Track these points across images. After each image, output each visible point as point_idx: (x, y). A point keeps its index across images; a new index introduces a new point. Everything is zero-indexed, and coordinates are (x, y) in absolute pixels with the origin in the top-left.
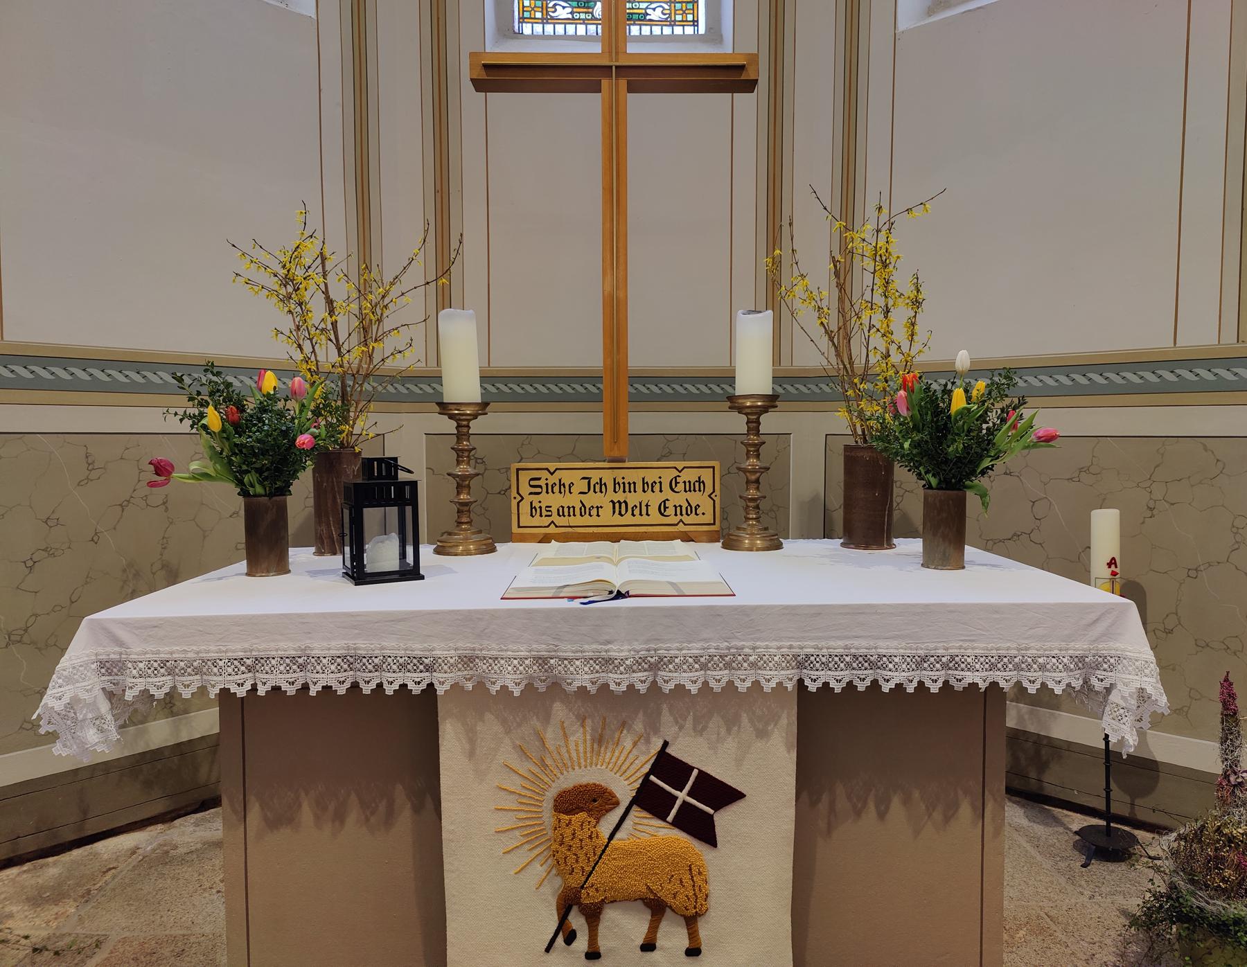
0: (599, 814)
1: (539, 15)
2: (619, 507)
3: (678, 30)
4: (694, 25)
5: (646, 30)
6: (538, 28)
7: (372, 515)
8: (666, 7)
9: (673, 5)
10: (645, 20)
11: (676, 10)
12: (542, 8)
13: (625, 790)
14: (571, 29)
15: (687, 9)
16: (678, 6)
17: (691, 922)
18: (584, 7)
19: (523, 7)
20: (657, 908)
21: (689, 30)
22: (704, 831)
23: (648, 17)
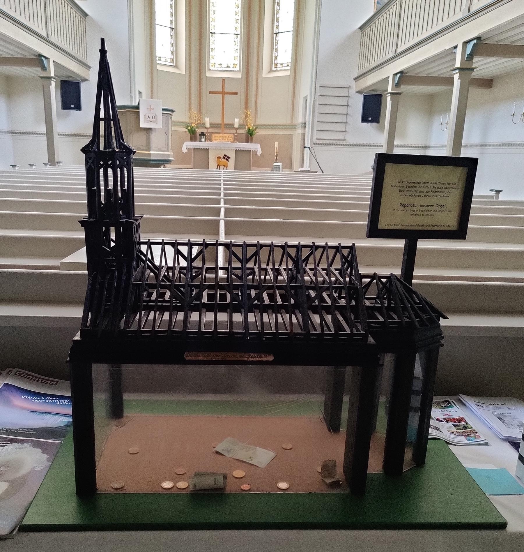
0: (220, 159)
2: (223, 139)
7: (202, 137)
13: (222, 157)
17: (227, 167)
20: (224, 166)
22: (227, 160)
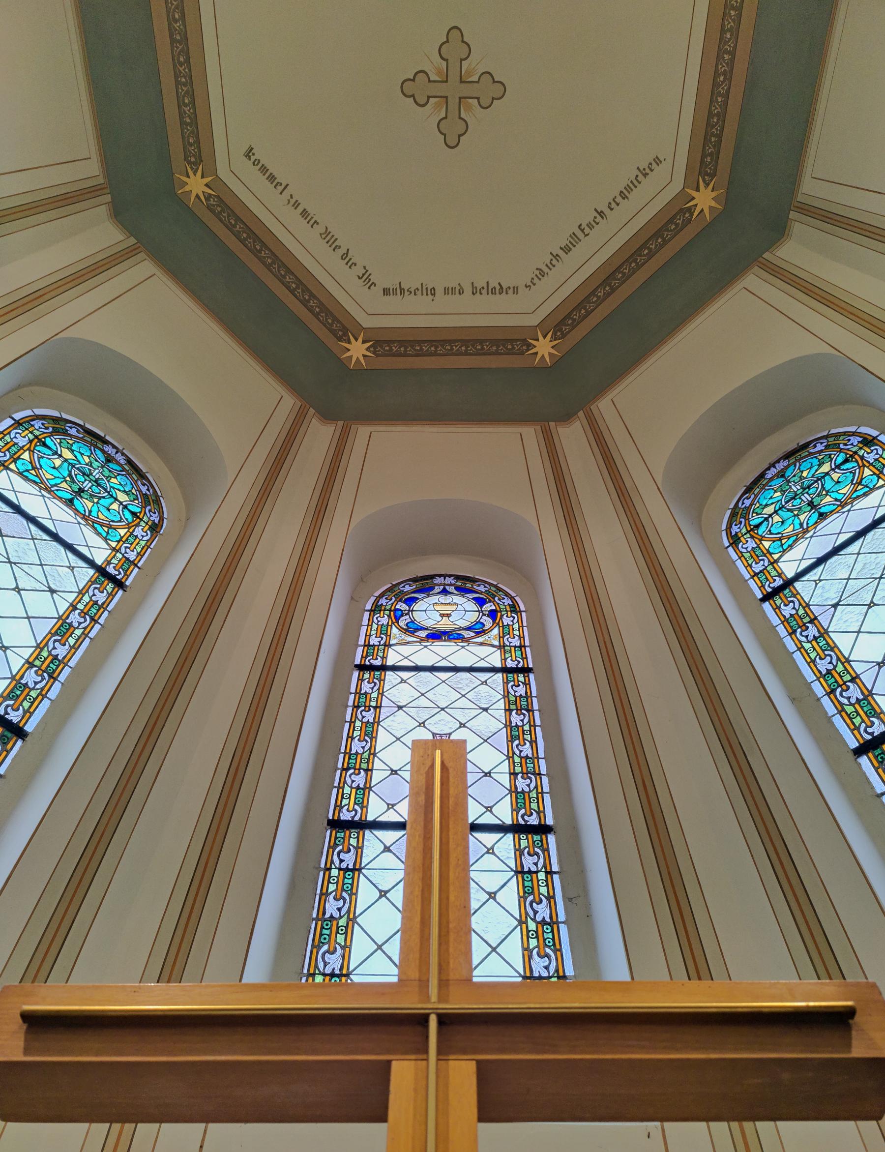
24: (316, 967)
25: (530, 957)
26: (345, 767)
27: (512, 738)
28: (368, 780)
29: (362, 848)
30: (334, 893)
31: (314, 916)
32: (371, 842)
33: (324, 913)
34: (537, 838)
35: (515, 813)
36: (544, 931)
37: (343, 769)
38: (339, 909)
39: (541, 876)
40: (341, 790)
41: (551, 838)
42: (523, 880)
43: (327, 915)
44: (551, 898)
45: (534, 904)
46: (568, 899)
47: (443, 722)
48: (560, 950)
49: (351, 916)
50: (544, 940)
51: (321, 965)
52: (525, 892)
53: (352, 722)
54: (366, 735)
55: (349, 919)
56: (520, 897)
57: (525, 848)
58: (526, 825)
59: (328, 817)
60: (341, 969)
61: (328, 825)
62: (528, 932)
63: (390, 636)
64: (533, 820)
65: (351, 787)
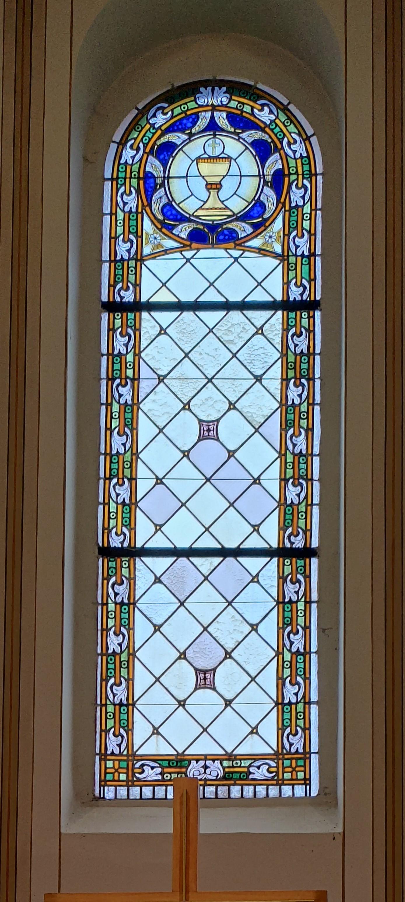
1: (123, 777)
3: (287, 791)
4: (306, 785)
5: (249, 791)
6: (123, 792)
8: (273, 764)
9: (280, 762)
10: (247, 779)
11: (284, 768)
12: (127, 768)
14: (160, 792)
15: (297, 766)
16: (287, 763)
18: (176, 767)
19: (106, 768)
21: (300, 791)
23: (251, 776)
24: (107, 697)
25: (284, 684)
26: (108, 476)
27: (286, 425)
28: (133, 492)
29: (134, 579)
30: (113, 628)
31: (99, 651)
32: (142, 572)
33: (107, 649)
34: (301, 563)
35: (282, 532)
36: (297, 661)
37: (105, 479)
38: (120, 645)
39: (301, 606)
40: (106, 507)
41: (314, 561)
42: (284, 610)
43: (110, 651)
44: (307, 628)
45: (292, 635)
46: (321, 630)
47: (210, 402)
48: (309, 679)
49: (131, 651)
50: (297, 669)
51: (111, 697)
52: (284, 623)
53: (108, 405)
54: (126, 425)
55: (129, 654)
56: (279, 629)
57: (288, 576)
58: (291, 548)
59: (98, 544)
60: (128, 699)
61: (100, 553)
62: (283, 662)
63: (142, 236)
64: (299, 543)
65: (117, 503)
